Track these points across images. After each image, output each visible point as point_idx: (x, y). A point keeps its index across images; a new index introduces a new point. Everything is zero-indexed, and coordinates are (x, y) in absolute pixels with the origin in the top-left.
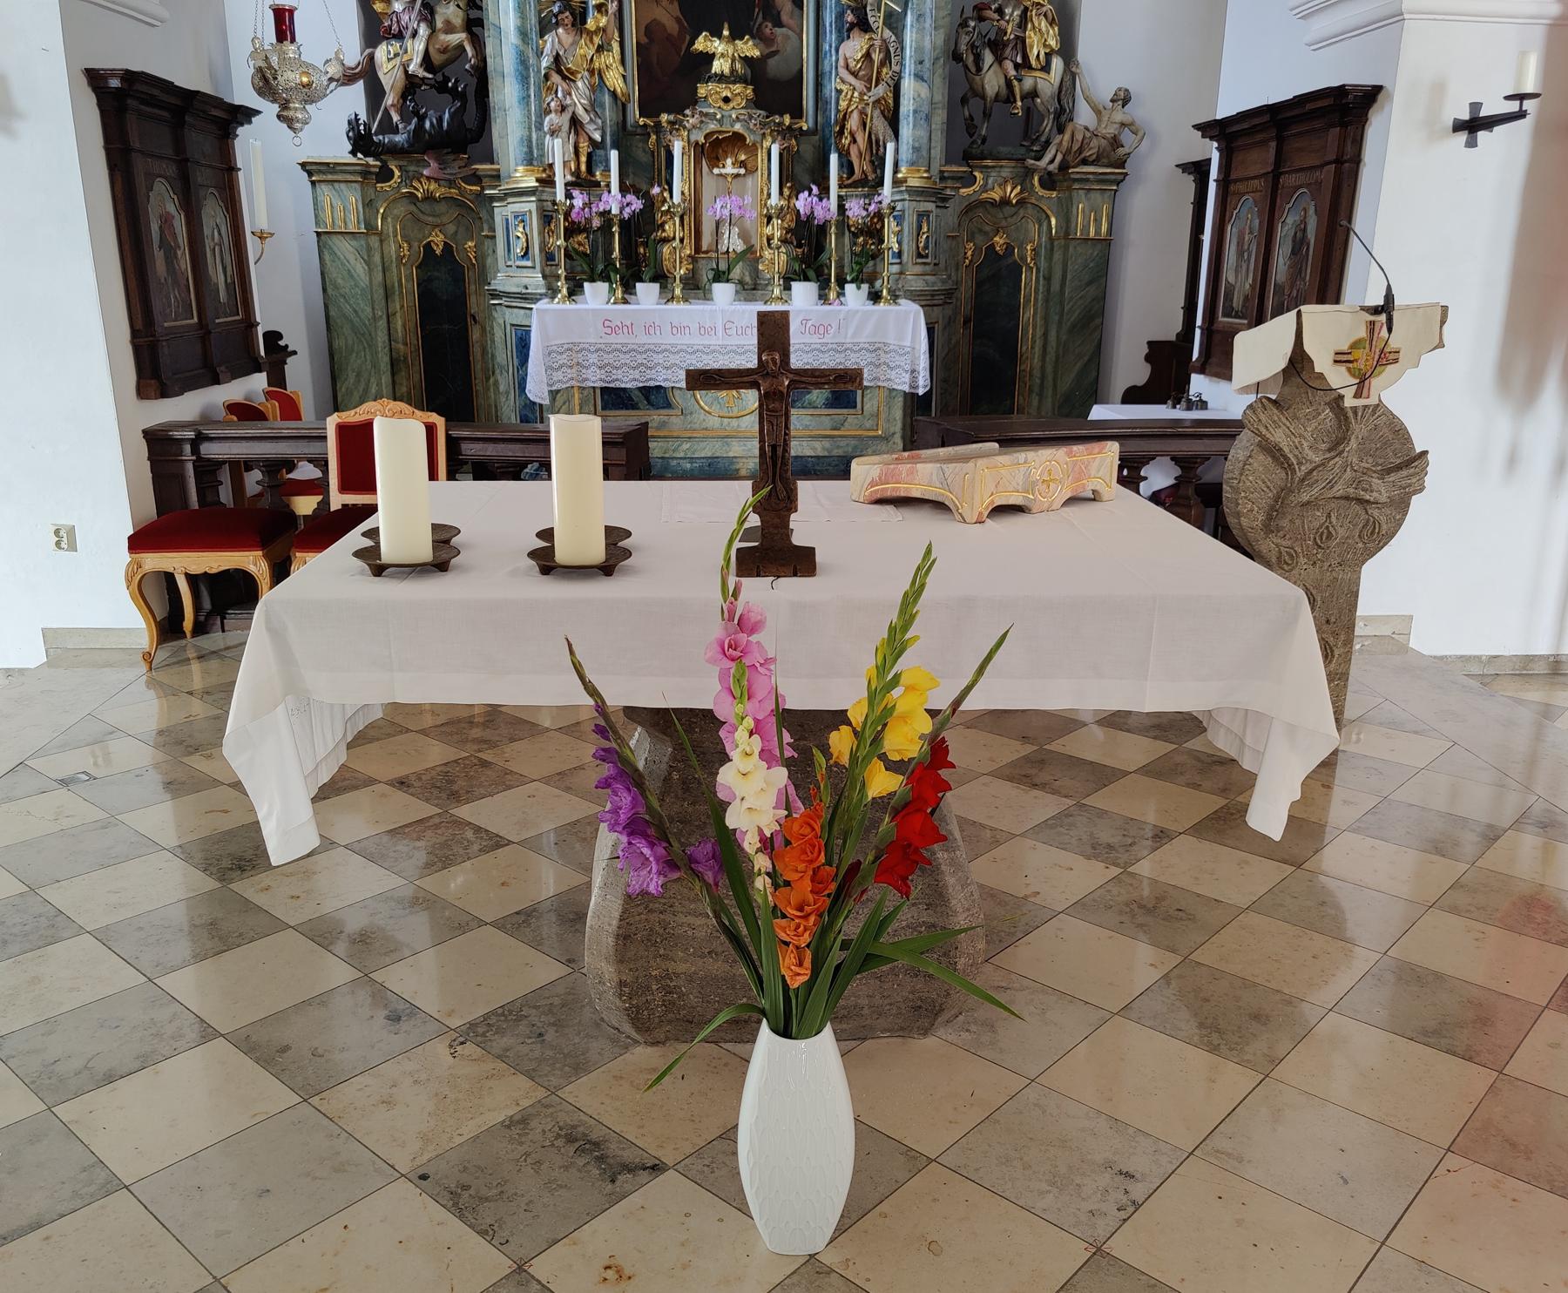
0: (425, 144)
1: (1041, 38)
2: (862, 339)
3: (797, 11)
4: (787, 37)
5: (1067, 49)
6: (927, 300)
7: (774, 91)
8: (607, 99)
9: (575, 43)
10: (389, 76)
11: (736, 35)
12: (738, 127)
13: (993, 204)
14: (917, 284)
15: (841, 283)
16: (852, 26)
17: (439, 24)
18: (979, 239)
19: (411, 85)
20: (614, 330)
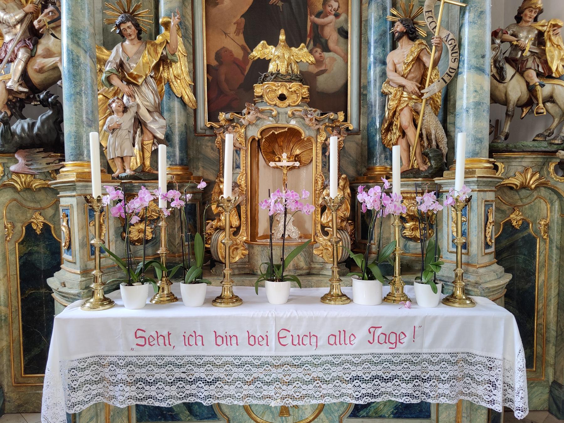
2: (444, 348)
3: (342, 40)
4: (334, 60)
8: (176, 105)
9: (139, 53)
11: (292, 43)
12: (293, 123)
16: (402, 34)
17: (40, 50)
20: (148, 341)
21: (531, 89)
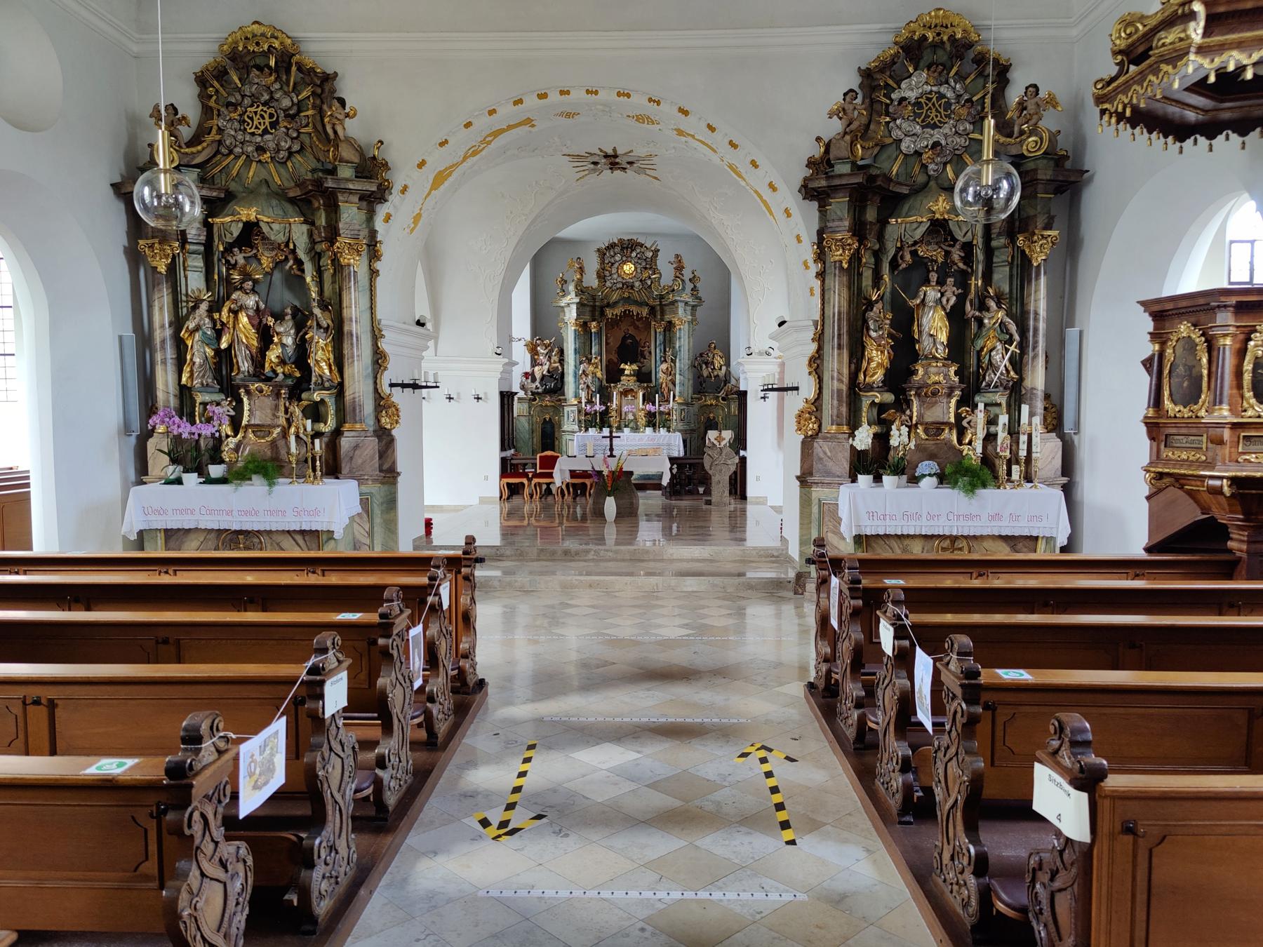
0: (546, 392)
1: (718, 361)
5: (728, 364)
6: (683, 432)
7: (643, 377)
10: (538, 376)
19: (543, 377)
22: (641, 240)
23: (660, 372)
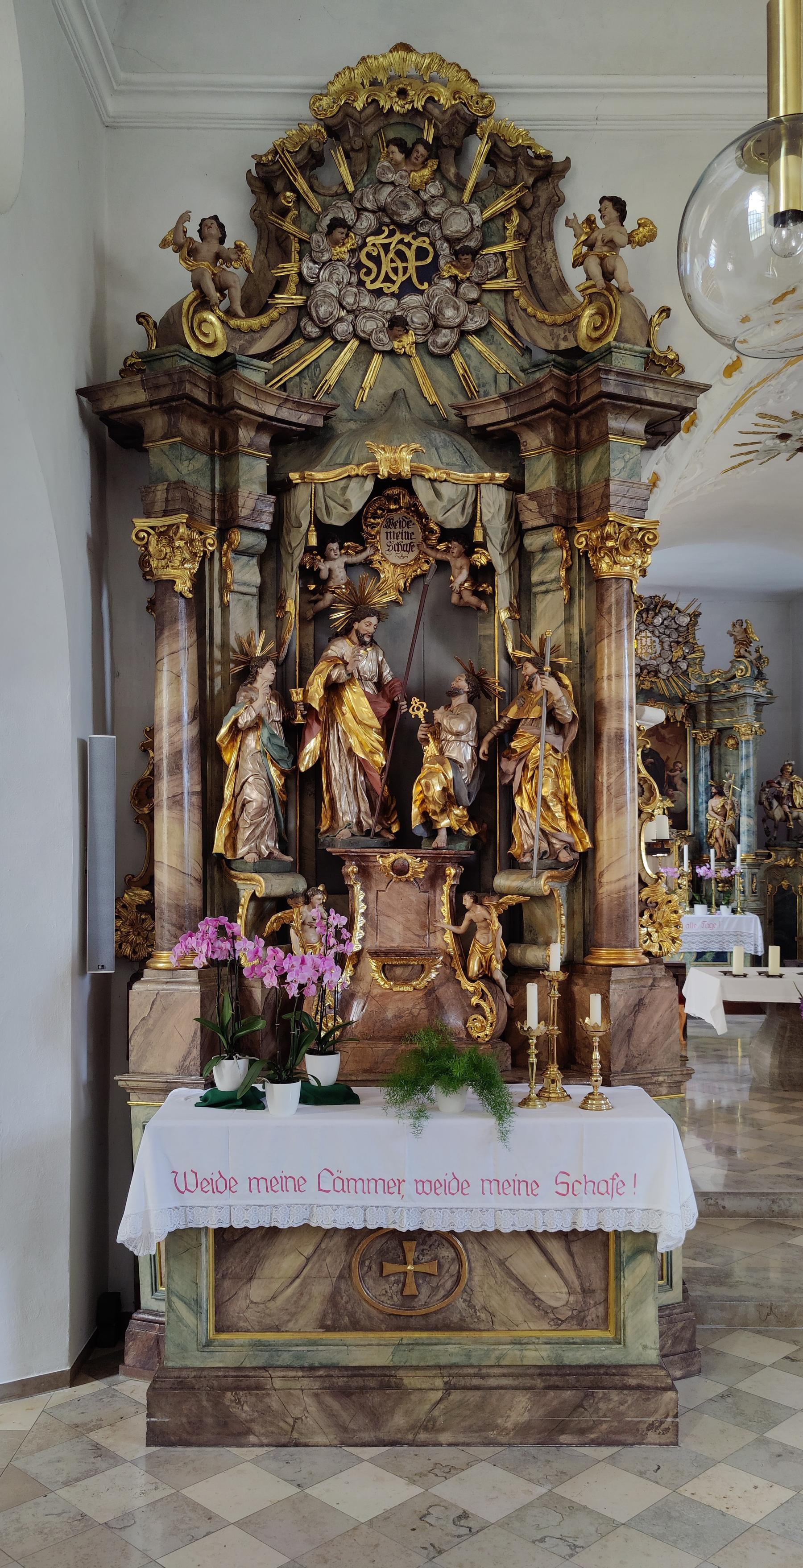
2: (731, 930)
13: (781, 867)
14: (753, 905)
15: (718, 905)
18: (774, 882)
21: (786, 814)
22: (671, 598)
23: (711, 814)
